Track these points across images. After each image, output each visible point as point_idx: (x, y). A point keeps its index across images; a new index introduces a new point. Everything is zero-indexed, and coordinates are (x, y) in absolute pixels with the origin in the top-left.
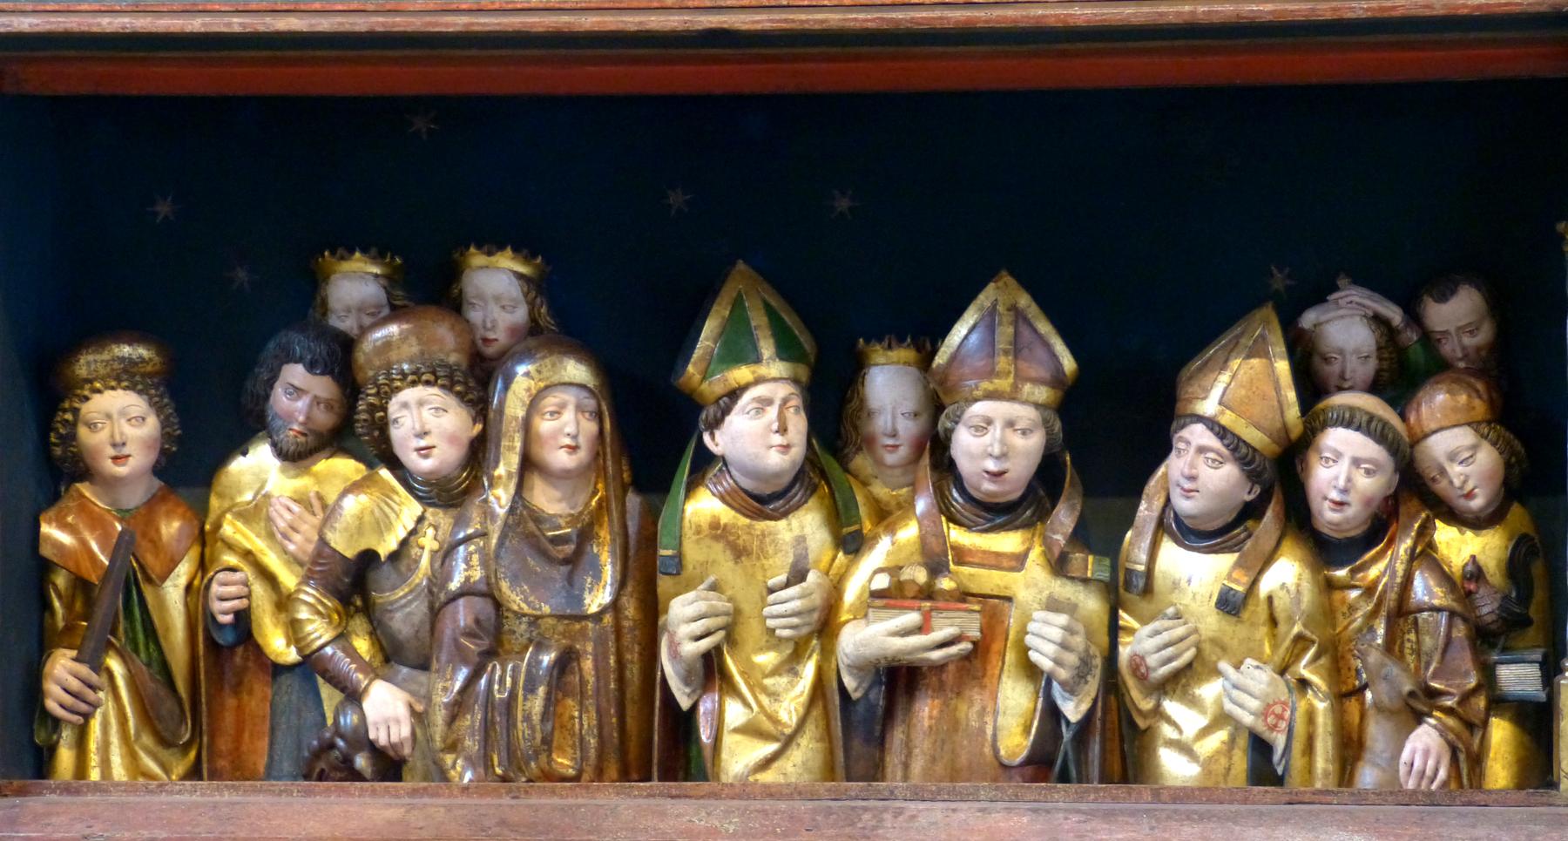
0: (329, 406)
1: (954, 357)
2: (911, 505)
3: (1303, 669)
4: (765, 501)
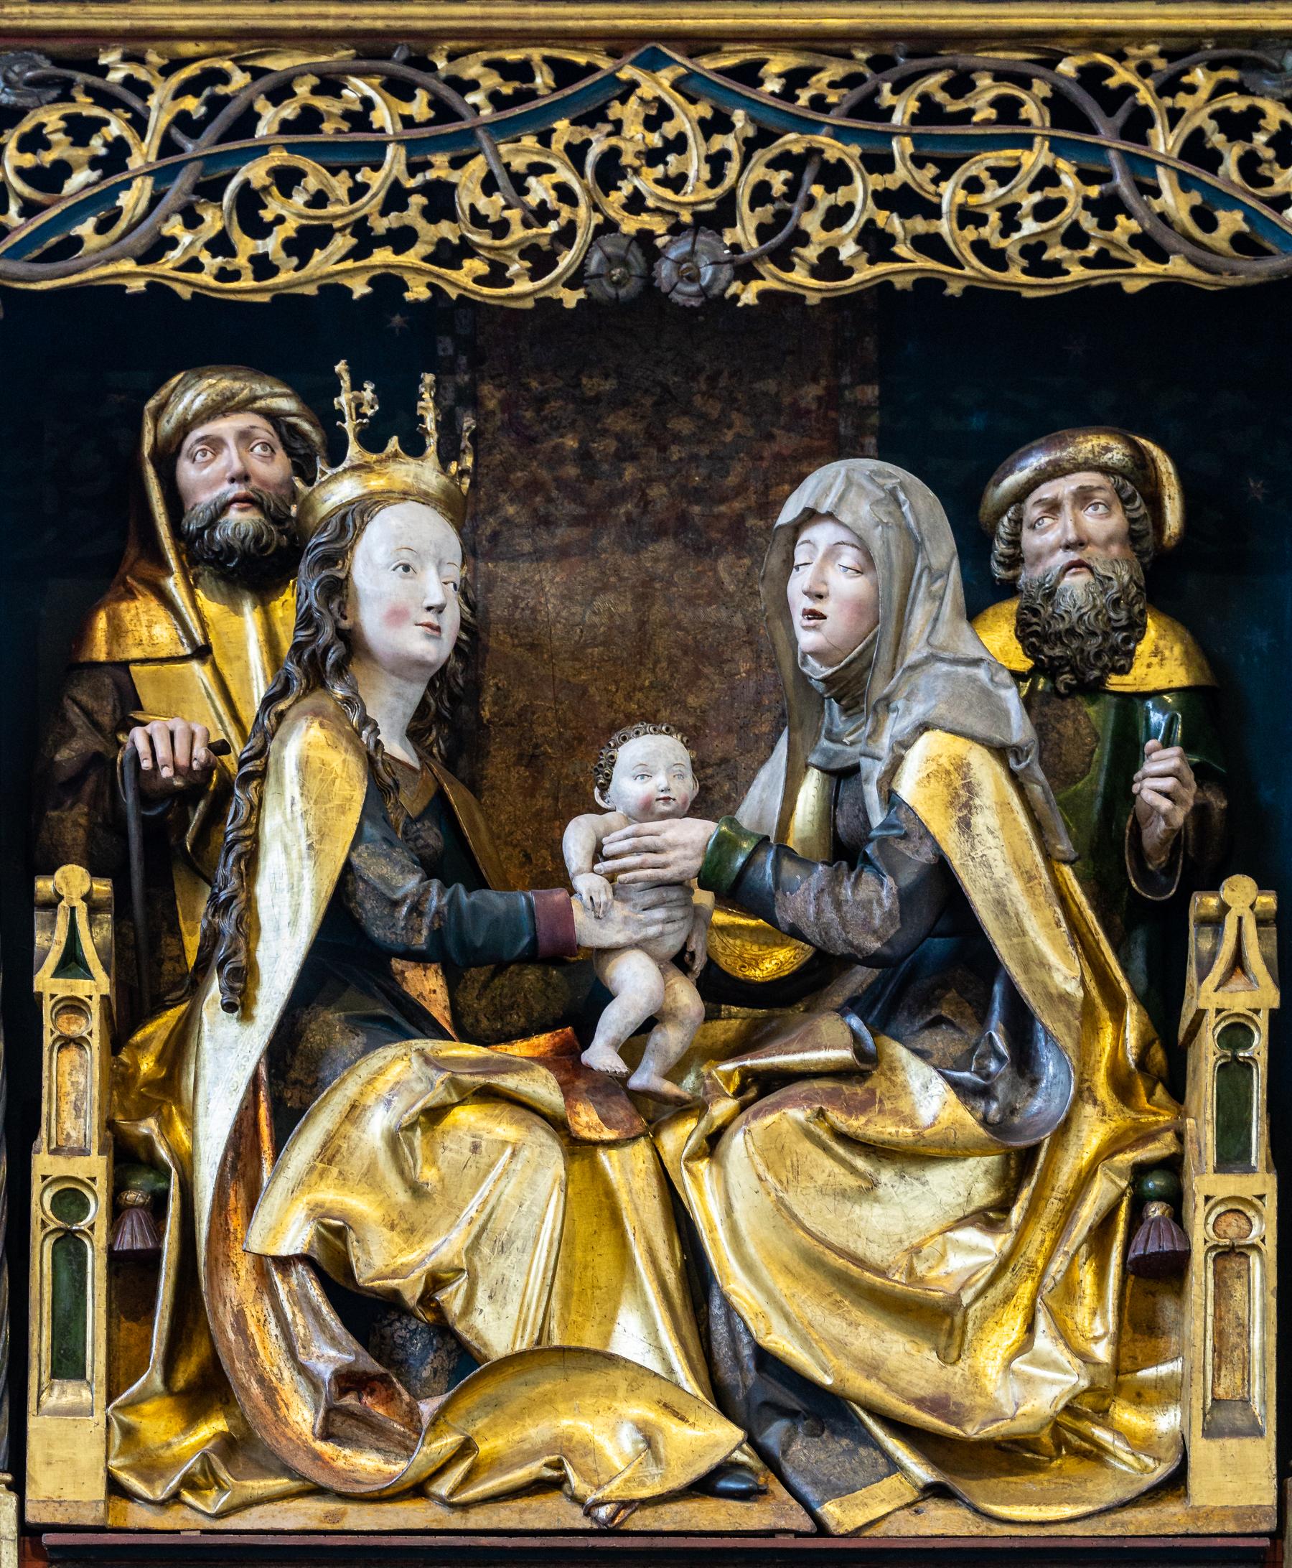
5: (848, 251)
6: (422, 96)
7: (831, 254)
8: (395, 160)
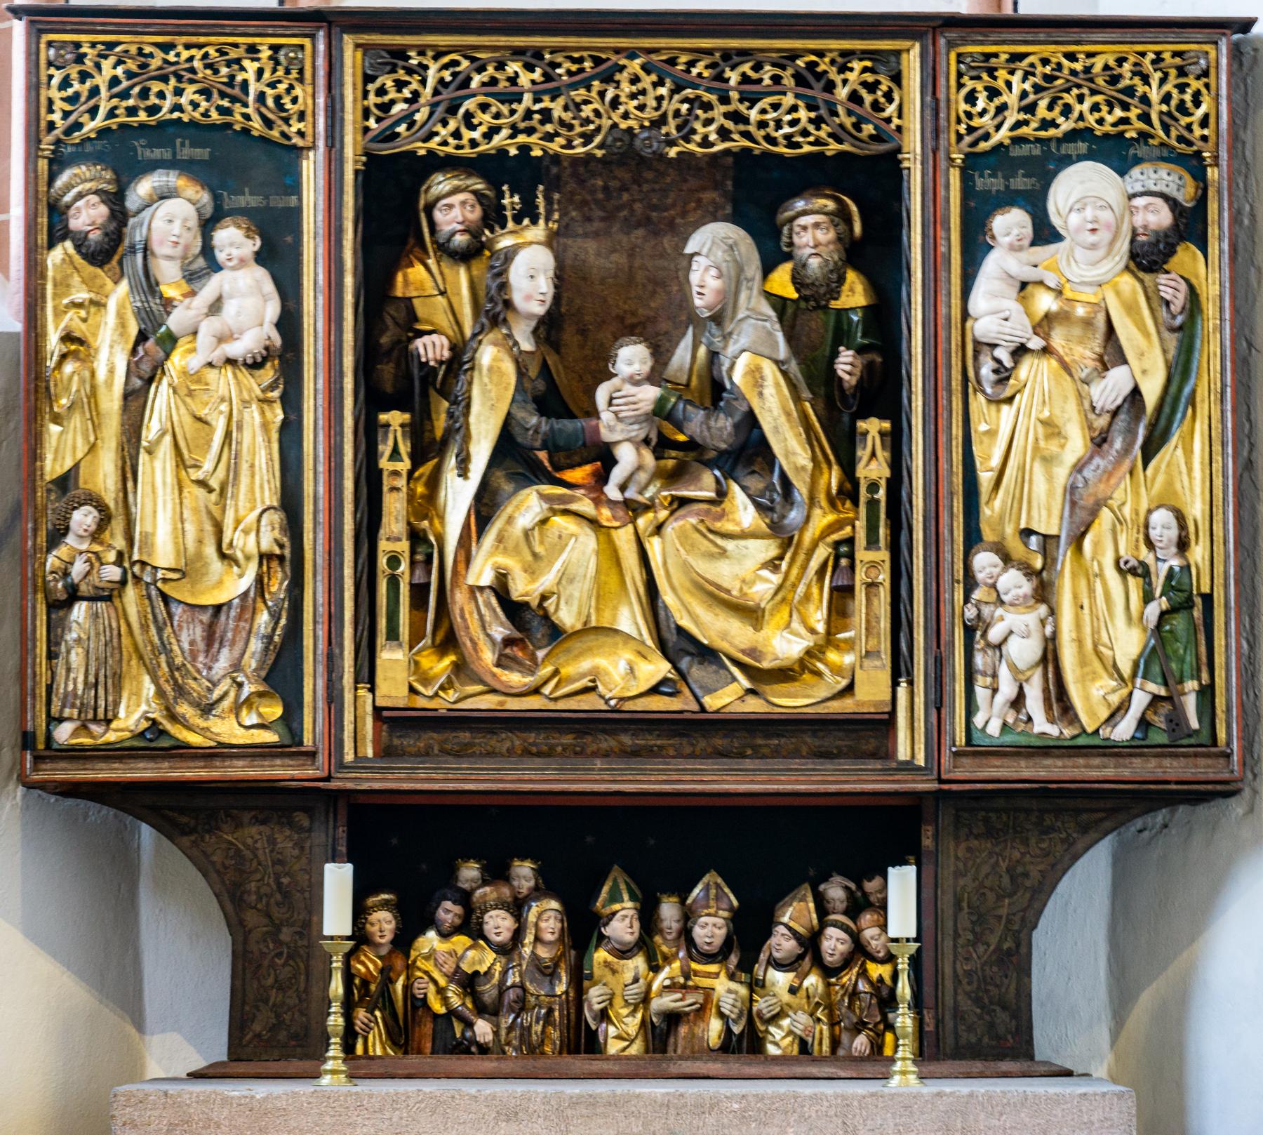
0: (460, 916)
1: (694, 901)
2: (677, 953)
3: (819, 1014)
4: (624, 953)
5: (713, 137)
6: (539, 71)
7: (705, 137)
8: (527, 98)
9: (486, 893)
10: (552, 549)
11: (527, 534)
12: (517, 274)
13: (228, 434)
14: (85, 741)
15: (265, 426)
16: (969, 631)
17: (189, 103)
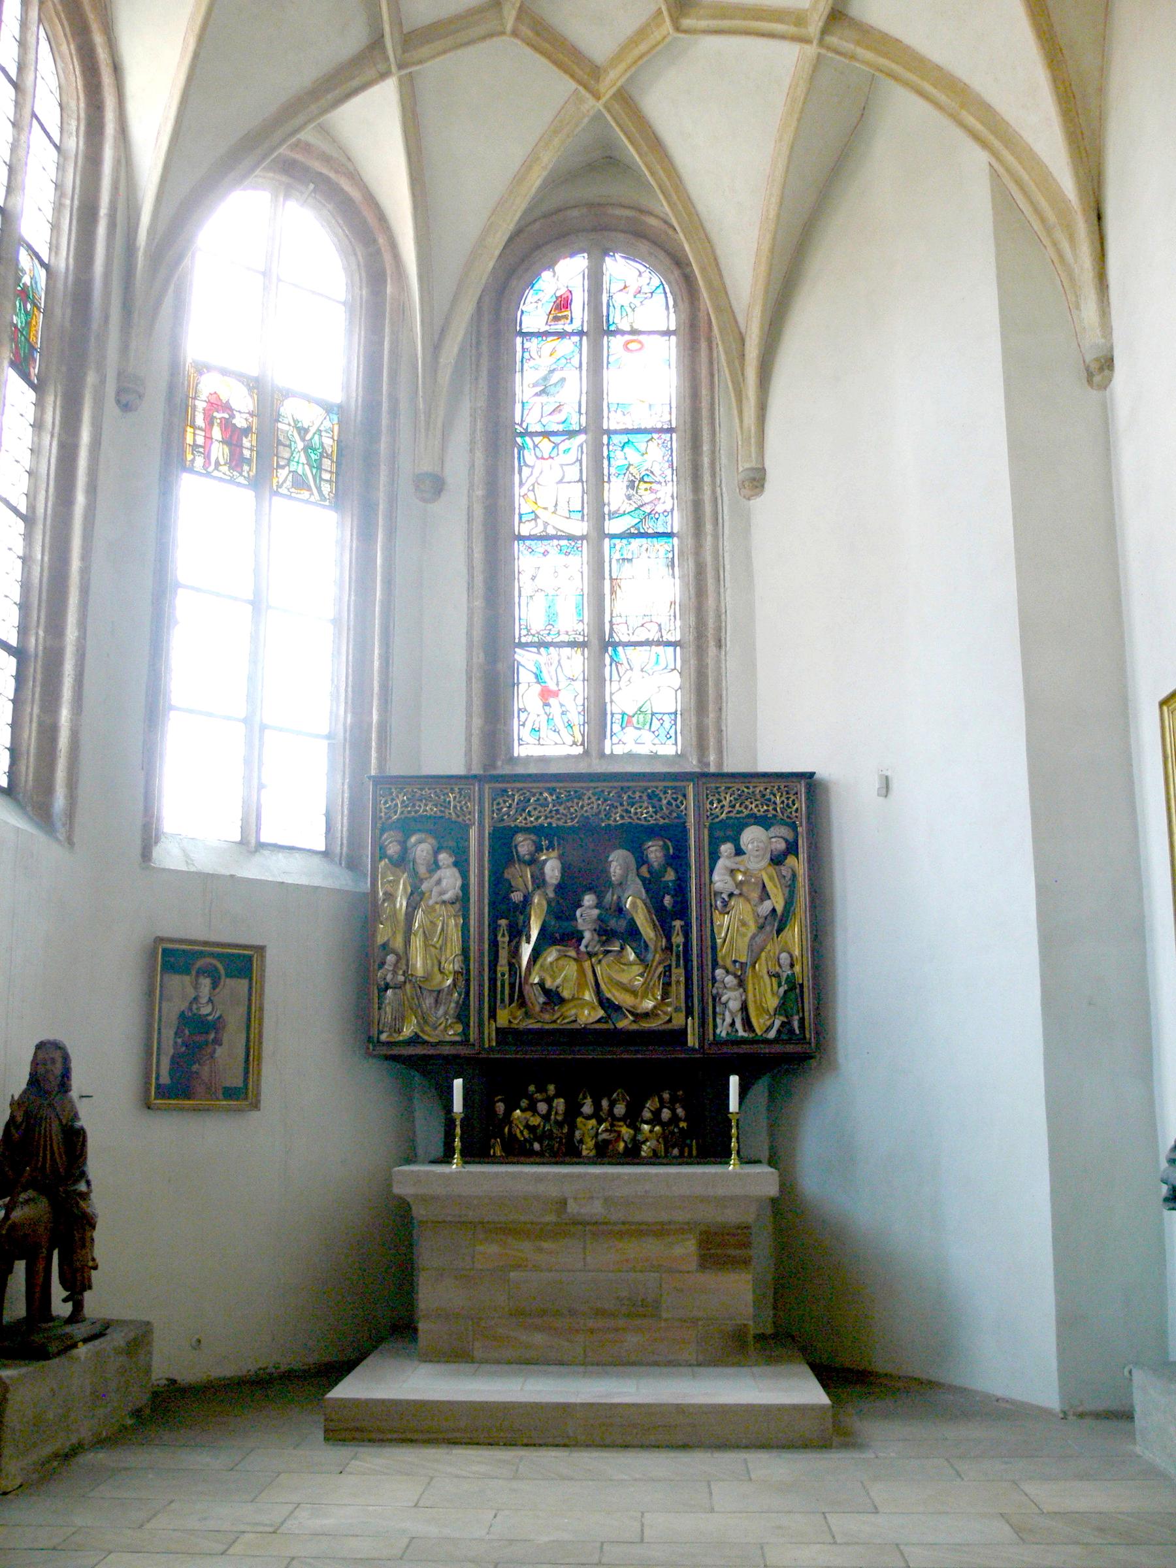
4: (588, 1118)
9: (538, 1096)
10: (560, 970)
11: (551, 963)
12: (548, 868)
13: (442, 930)
14: (392, 1040)
15: (456, 925)
16: (714, 999)
17: (430, 809)
